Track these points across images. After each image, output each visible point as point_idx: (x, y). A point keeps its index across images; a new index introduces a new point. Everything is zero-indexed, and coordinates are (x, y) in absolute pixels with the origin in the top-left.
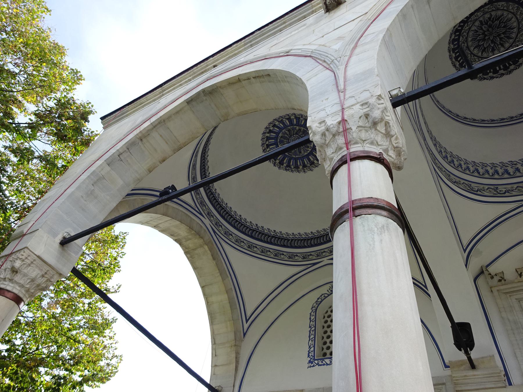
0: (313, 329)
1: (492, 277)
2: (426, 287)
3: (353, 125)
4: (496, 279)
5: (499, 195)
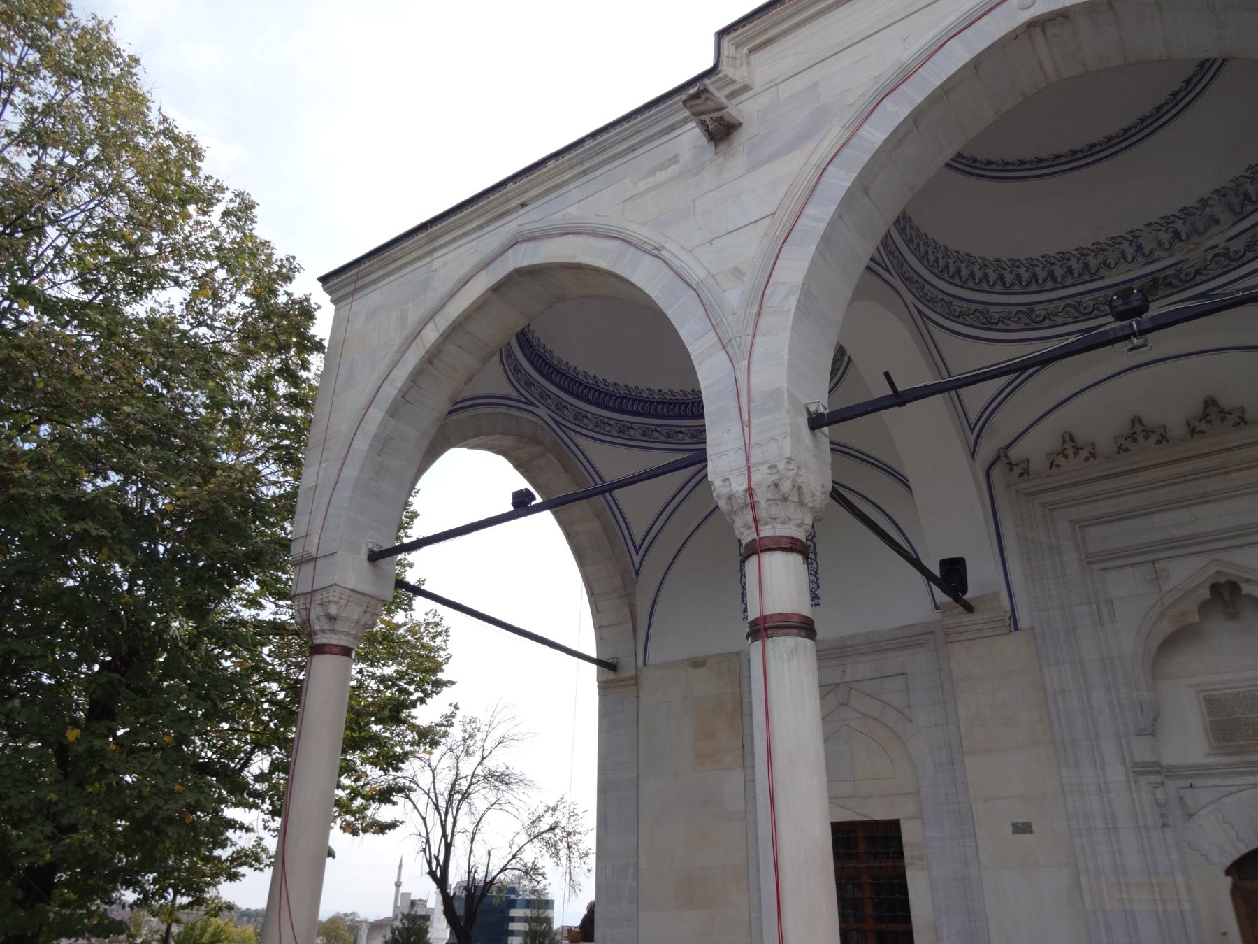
1: (1011, 470)
3: (760, 496)
4: (1017, 470)
5: (1033, 326)
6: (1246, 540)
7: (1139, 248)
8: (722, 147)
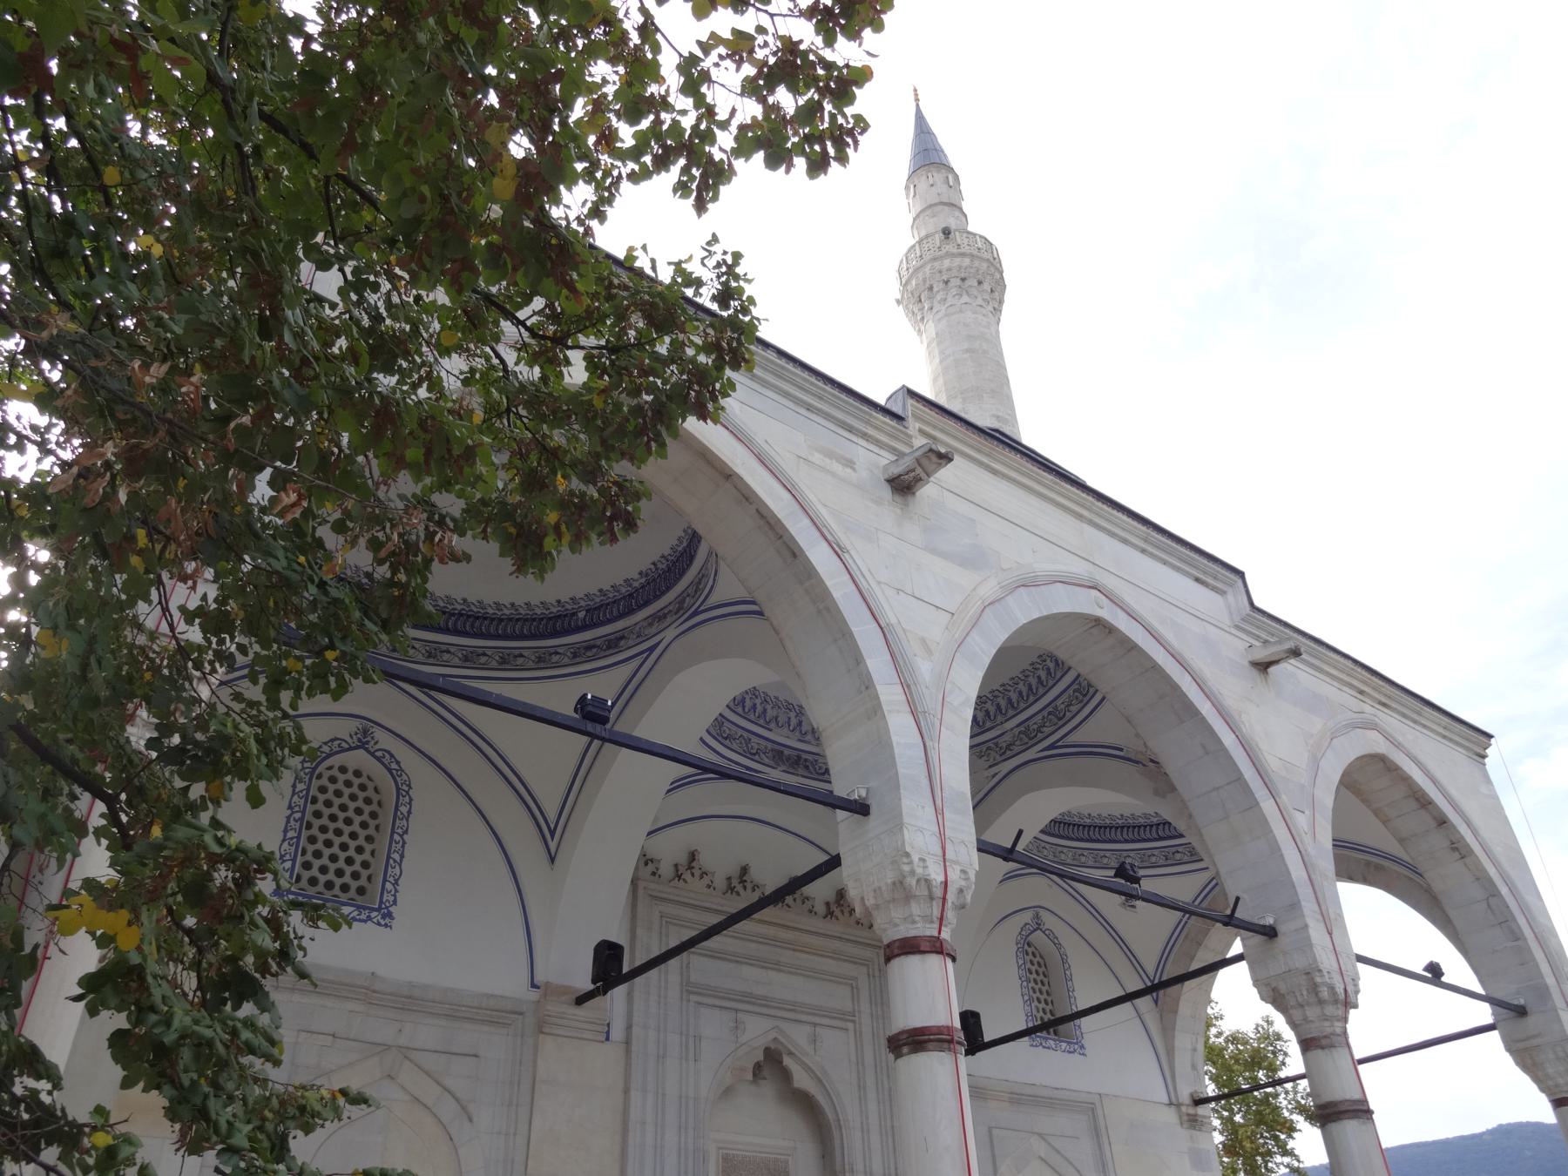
0: (298, 815)
2: (552, 834)
3: (951, 897)
4: (651, 867)
6: (799, 1017)
7: (800, 724)
8: (898, 498)
